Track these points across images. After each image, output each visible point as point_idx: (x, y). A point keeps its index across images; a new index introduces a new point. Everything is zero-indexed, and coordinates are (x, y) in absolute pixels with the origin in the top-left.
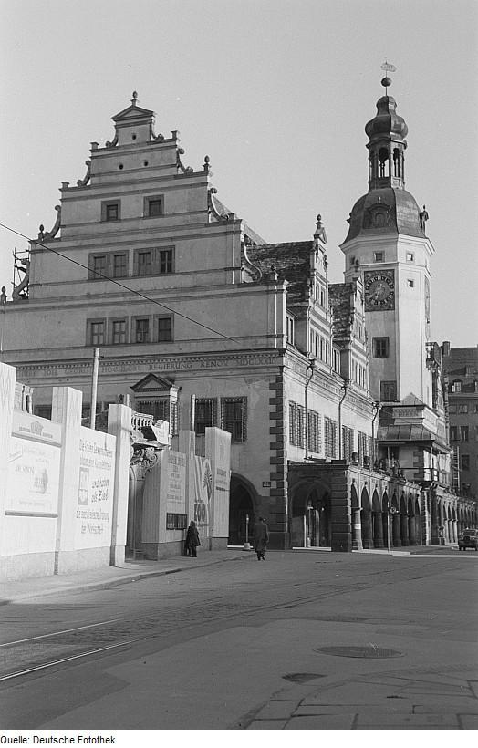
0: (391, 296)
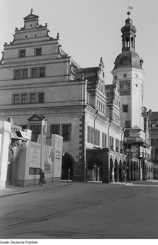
0: (129, 90)
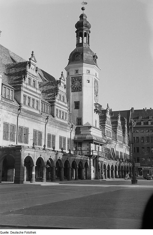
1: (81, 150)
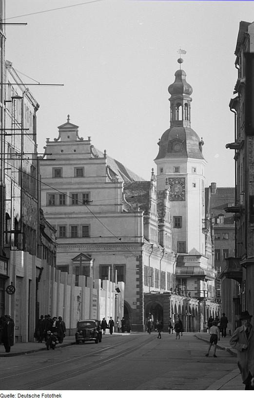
0: (183, 193)
1: (186, 291)
